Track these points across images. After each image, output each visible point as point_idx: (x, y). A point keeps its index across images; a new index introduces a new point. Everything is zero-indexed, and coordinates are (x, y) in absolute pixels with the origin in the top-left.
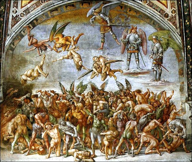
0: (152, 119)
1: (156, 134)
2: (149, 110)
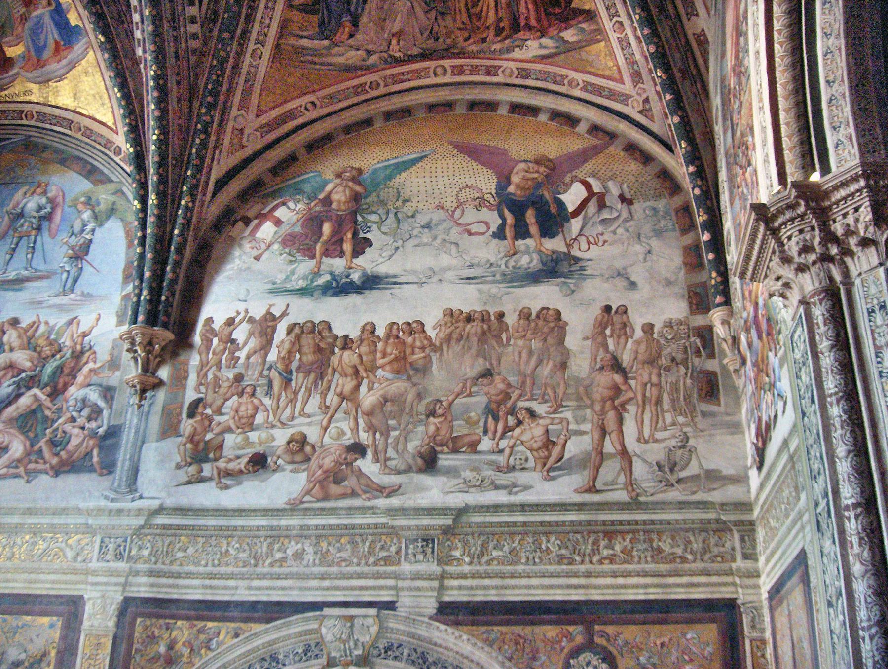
0: (29, 388)
1: (29, 425)
2: (28, 364)
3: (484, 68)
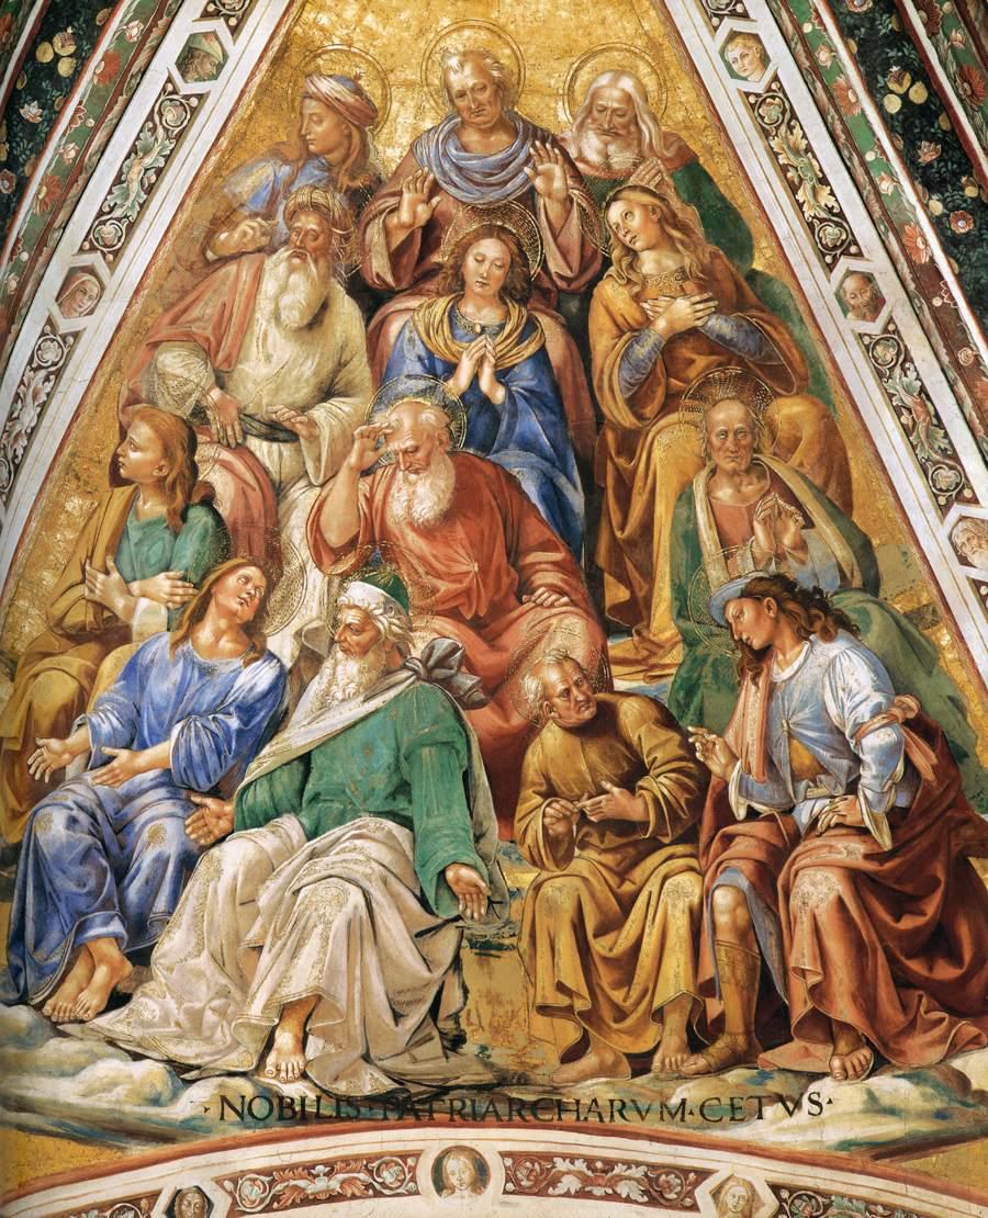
3: (638, 1172)
